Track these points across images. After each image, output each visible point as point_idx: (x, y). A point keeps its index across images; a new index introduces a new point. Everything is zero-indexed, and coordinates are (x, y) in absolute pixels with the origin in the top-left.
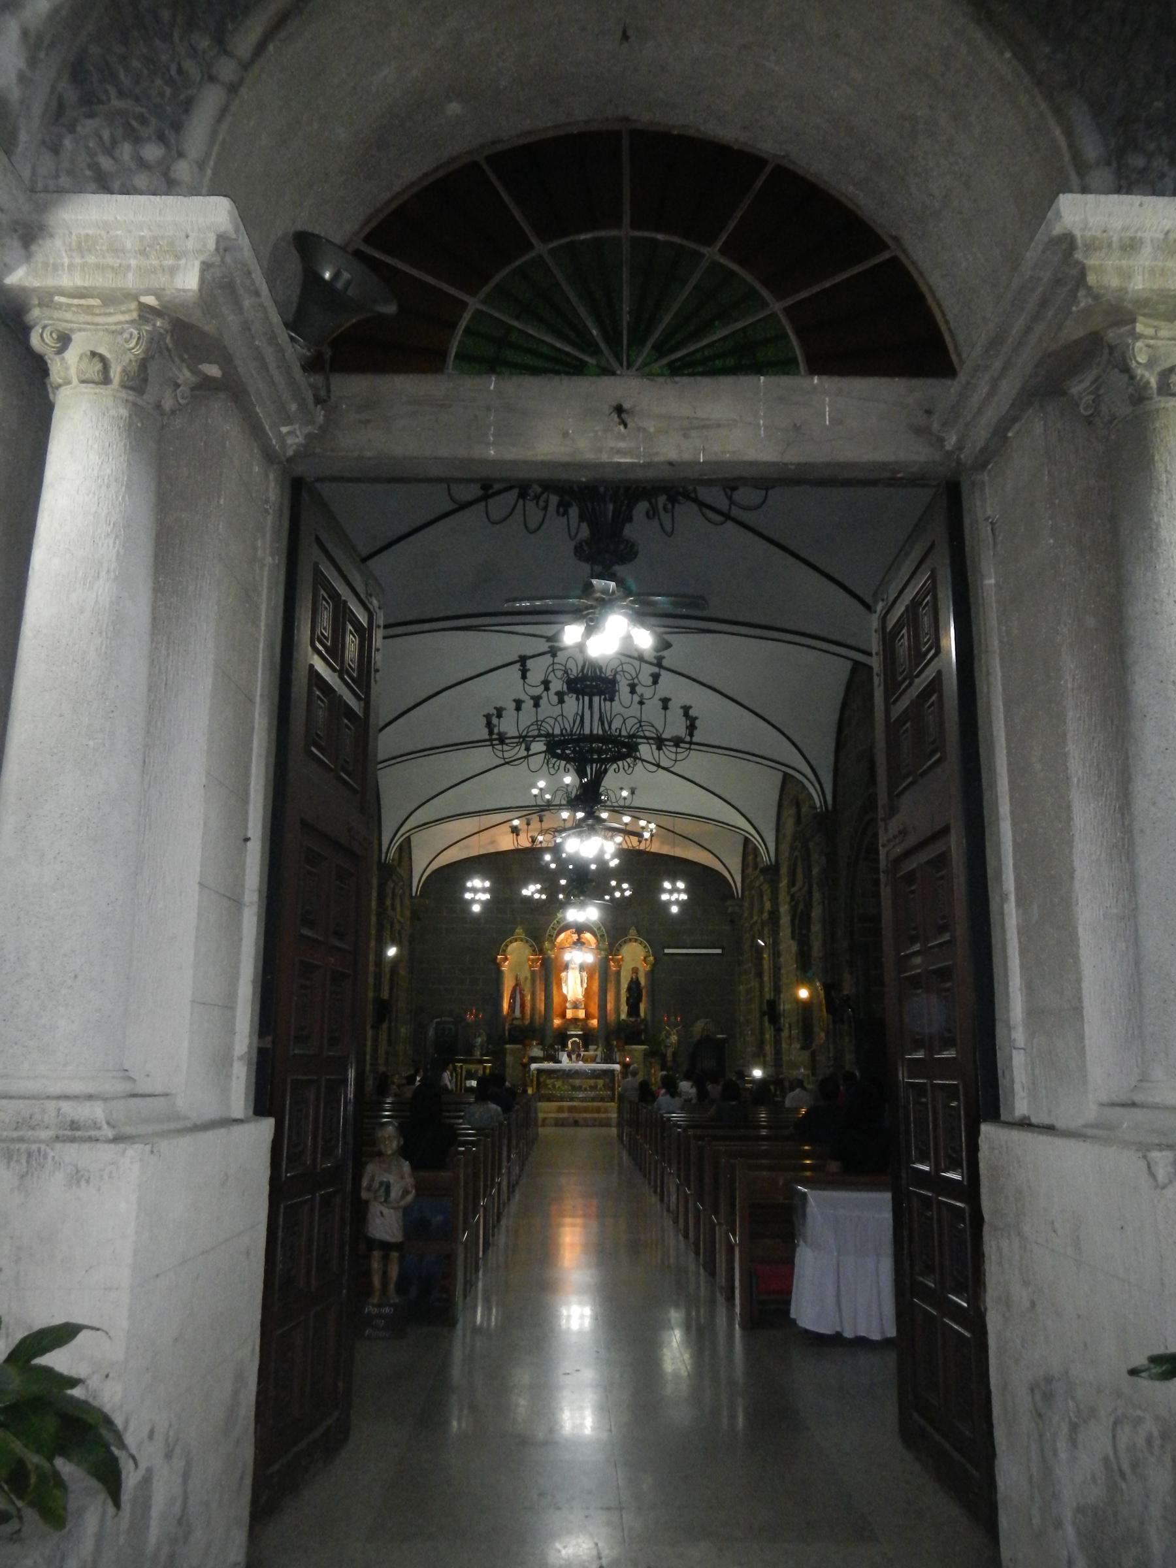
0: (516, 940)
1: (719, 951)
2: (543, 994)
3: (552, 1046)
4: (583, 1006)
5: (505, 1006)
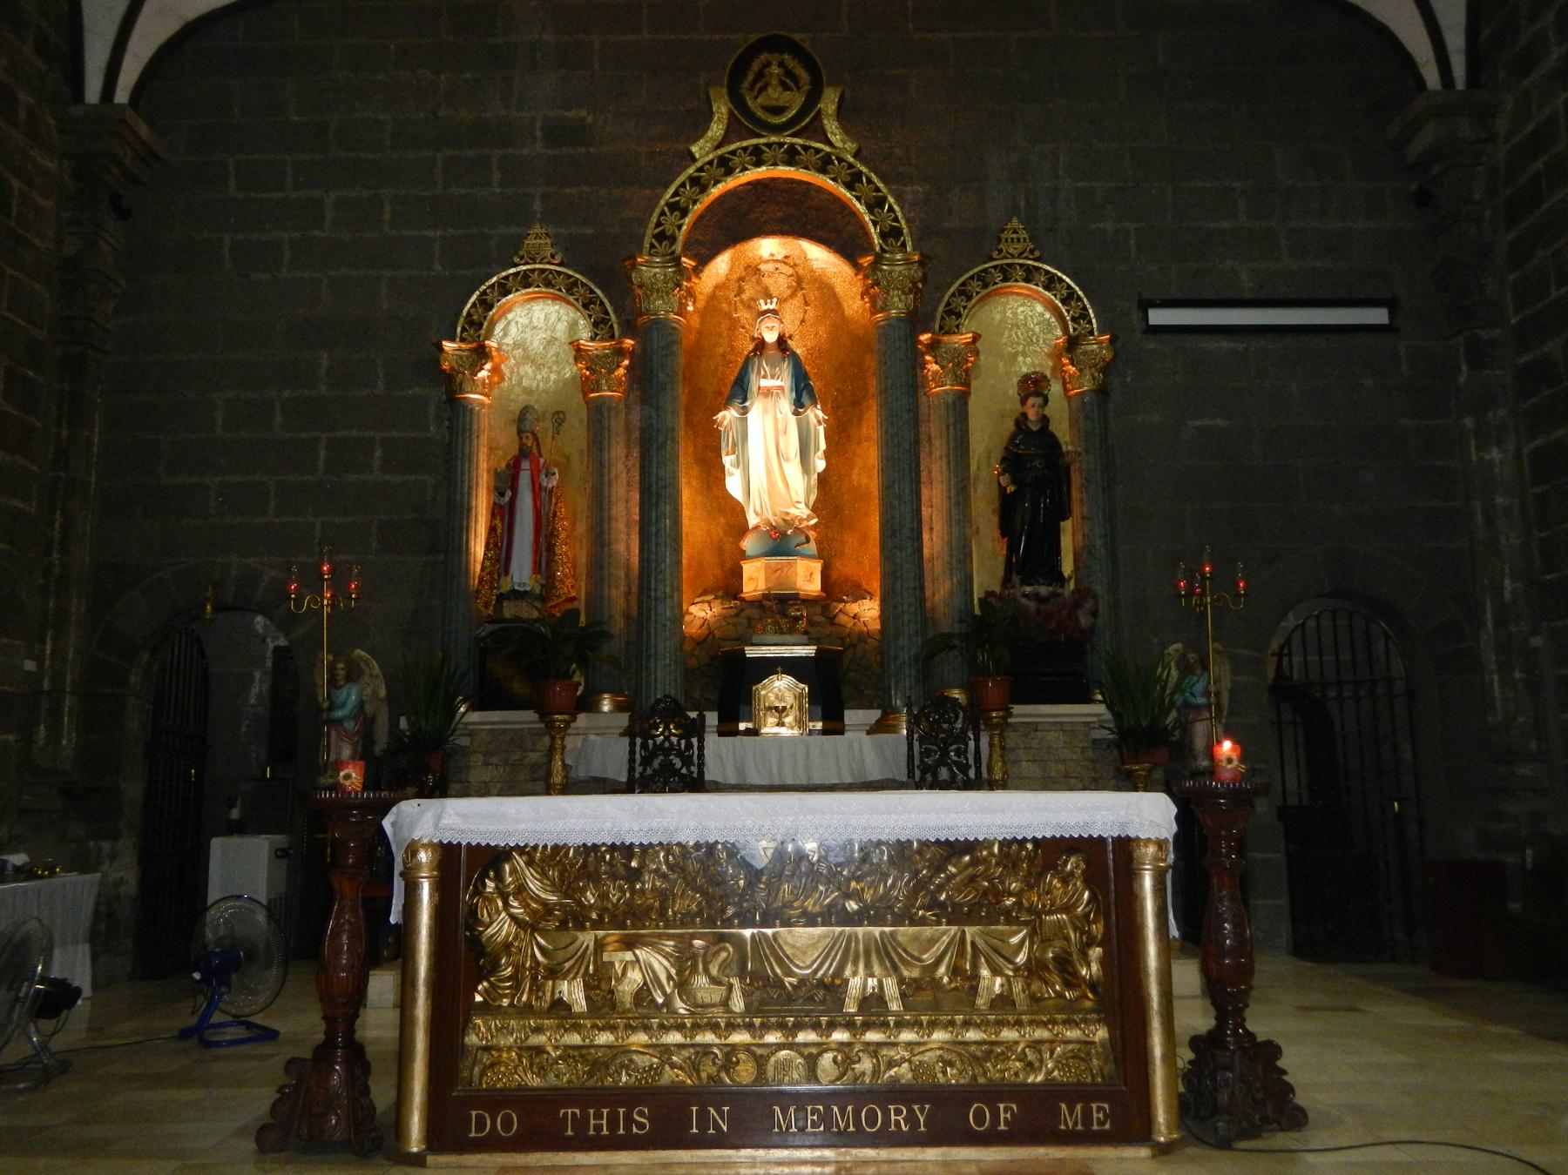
0: (525, 281)
1: (1379, 316)
2: (636, 496)
3: (672, 711)
4: (812, 547)
5: (478, 548)
